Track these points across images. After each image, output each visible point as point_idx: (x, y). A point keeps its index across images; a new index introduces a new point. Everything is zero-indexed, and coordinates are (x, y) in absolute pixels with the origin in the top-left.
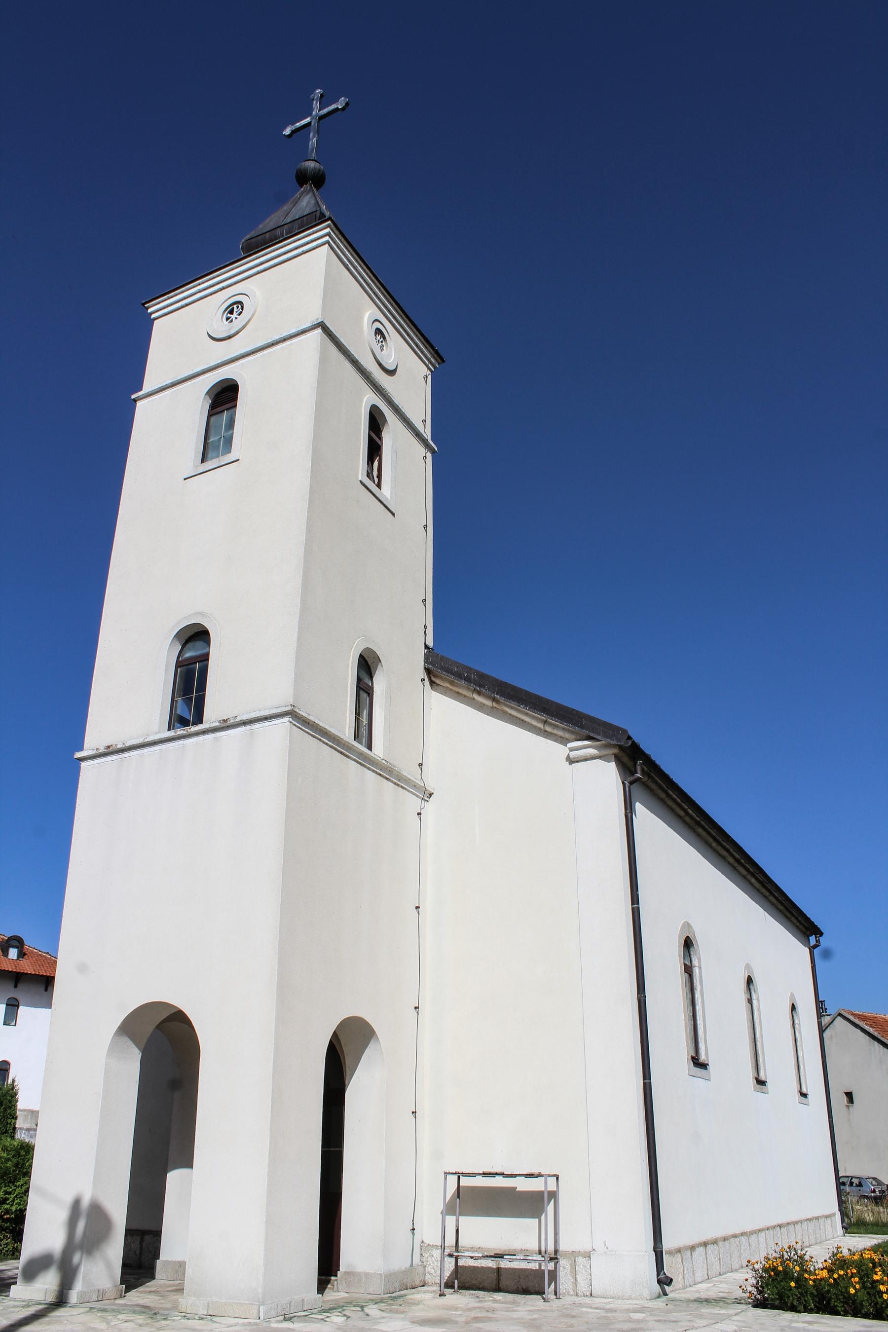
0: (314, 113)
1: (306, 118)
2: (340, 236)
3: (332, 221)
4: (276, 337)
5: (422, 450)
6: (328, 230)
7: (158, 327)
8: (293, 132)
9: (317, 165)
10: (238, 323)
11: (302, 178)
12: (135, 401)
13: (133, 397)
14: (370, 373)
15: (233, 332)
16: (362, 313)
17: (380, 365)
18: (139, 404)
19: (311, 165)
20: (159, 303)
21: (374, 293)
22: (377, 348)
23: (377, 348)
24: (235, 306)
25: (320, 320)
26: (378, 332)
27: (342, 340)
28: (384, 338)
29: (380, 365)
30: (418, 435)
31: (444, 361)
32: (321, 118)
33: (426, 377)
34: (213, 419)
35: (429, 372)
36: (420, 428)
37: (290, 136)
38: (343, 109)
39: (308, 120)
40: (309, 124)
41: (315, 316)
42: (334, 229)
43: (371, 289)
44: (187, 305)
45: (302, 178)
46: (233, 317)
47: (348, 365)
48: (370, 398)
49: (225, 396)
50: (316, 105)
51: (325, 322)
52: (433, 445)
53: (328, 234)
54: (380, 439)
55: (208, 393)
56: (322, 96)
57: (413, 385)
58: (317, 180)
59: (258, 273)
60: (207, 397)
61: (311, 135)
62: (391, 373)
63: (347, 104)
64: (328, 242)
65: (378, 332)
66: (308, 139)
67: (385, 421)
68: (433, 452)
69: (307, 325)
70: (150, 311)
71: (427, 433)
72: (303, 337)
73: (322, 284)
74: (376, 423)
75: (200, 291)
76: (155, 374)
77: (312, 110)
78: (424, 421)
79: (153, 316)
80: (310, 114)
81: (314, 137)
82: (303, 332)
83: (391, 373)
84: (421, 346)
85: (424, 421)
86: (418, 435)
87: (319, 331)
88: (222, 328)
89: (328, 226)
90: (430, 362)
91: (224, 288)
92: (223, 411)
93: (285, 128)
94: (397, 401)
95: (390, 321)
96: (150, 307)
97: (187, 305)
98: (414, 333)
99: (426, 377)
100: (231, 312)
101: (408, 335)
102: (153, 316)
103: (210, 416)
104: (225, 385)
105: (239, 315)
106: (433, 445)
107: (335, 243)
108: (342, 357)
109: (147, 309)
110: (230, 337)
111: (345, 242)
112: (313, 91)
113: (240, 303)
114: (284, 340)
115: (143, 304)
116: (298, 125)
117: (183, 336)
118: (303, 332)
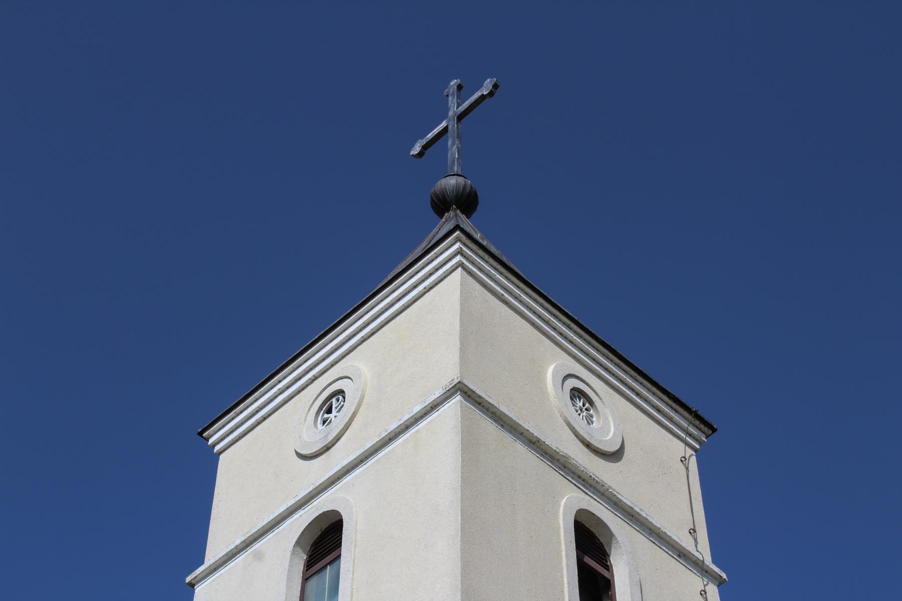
0: (451, 113)
1: (441, 123)
2: (481, 252)
3: (463, 231)
4: (393, 426)
5: (696, 582)
6: (457, 245)
7: (225, 463)
8: (425, 147)
9: (461, 180)
10: (338, 419)
11: (441, 205)
12: (192, 585)
13: (188, 579)
14: (566, 457)
15: (330, 438)
16: (542, 368)
17: (588, 445)
18: (198, 589)
19: (452, 181)
20: (224, 426)
21: (561, 334)
22: (579, 423)
23: (579, 423)
24: (334, 400)
25: (456, 381)
26: (576, 394)
27: (503, 409)
28: (591, 403)
29: (588, 445)
30: (682, 555)
31: (714, 430)
32: (461, 117)
33: (684, 460)
34: (313, 583)
35: (690, 452)
36: (687, 543)
37: (420, 154)
38: (491, 94)
39: (444, 124)
40: (445, 130)
41: (450, 374)
42: (468, 242)
43: (554, 329)
44: (264, 418)
45: (441, 205)
46: (331, 416)
47: (521, 449)
48: (570, 500)
49: (324, 543)
50: (452, 101)
51: (466, 382)
52: (717, 570)
53: (459, 252)
54: (608, 568)
55: (298, 543)
56: (460, 87)
57: (657, 471)
58: (467, 202)
59: (364, 340)
60: (299, 549)
61: (450, 143)
62: (615, 456)
63: (496, 86)
64: (460, 265)
65: (576, 394)
66: (446, 150)
67: (611, 535)
68: (720, 583)
69: (438, 393)
70: (211, 441)
71: (704, 551)
72: (435, 415)
73: (458, 328)
74: (590, 543)
75: (281, 392)
76: (220, 537)
77: (448, 109)
78: (693, 531)
79: (217, 448)
80: (445, 116)
81: (453, 144)
82: (434, 407)
83: (615, 456)
84: (667, 410)
85: (693, 531)
86: (682, 555)
87: (458, 398)
88: (313, 436)
89: (458, 239)
90: (690, 435)
91: (315, 378)
92: (325, 567)
93: (412, 146)
94: (627, 499)
95: (600, 377)
96: (212, 436)
97: (264, 418)
98: (649, 390)
99: (684, 460)
100: (329, 411)
101: (638, 394)
102: (217, 448)
103: (306, 579)
104: (325, 525)
105: (339, 411)
106: (717, 570)
107: (473, 263)
108: (507, 438)
109: (207, 440)
110: (327, 448)
111: (491, 261)
112: (446, 85)
113: (341, 392)
114: (406, 427)
115: (200, 434)
116: (430, 135)
117: (261, 469)
118: (434, 407)
